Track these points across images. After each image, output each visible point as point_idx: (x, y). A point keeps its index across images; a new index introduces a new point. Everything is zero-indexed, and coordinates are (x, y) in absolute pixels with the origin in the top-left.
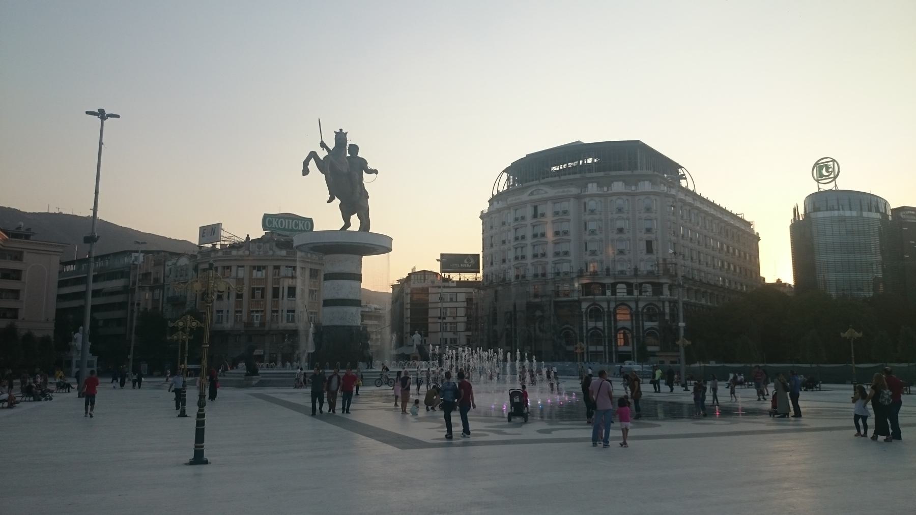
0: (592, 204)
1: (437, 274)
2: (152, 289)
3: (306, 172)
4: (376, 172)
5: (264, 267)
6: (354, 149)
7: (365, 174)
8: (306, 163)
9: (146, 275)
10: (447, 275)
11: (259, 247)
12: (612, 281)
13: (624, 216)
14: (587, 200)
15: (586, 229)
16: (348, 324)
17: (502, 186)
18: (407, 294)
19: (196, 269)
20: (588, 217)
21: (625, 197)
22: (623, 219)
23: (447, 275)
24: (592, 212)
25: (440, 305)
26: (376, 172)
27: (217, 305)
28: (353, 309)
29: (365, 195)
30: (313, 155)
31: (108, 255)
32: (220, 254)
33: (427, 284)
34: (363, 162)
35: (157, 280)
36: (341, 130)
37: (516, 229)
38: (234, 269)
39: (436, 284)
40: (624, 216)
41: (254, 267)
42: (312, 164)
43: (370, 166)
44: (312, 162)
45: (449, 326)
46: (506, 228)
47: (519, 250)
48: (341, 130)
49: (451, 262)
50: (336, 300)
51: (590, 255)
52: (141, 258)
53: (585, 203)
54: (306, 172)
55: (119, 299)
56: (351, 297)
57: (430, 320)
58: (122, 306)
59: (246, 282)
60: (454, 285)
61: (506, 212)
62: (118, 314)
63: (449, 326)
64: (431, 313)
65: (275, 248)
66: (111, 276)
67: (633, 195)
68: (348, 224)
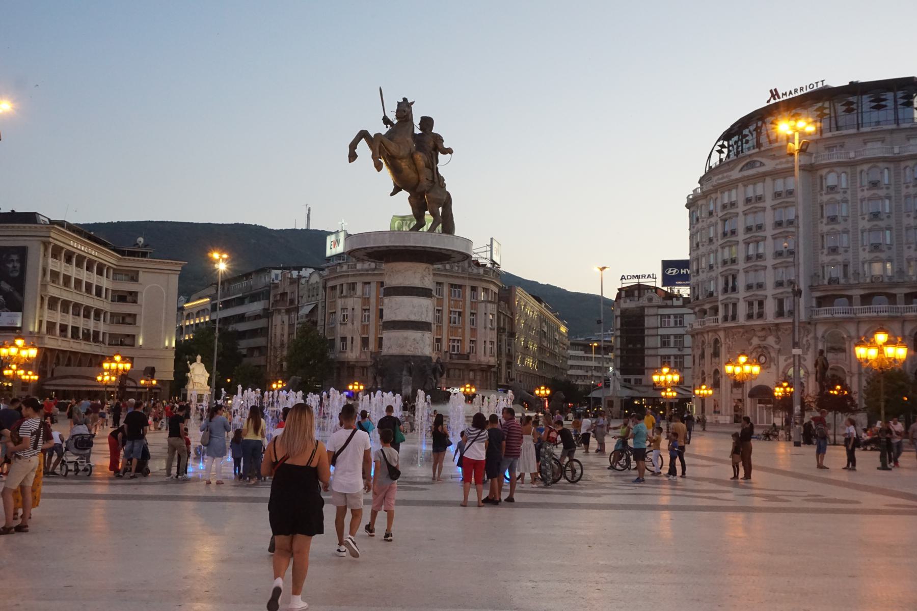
0: (831, 180)
1: (656, 288)
2: (288, 311)
3: (353, 157)
4: (449, 151)
6: (427, 123)
7: (440, 154)
8: (353, 146)
9: (284, 294)
10: (676, 290)
12: (862, 292)
13: (882, 193)
14: (824, 172)
15: (822, 216)
16: (409, 353)
17: (715, 160)
18: (616, 317)
19: (325, 288)
20: (825, 198)
21: (882, 165)
22: (880, 198)
23: (676, 290)
24: (832, 189)
25: (661, 331)
26: (449, 151)
27: (340, 331)
28: (417, 335)
29: (438, 182)
30: (363, 134)
31: (250, 274)
32: (345, 267)
33: (644, 302)
34: (438, 139)
35: (292, 301)
36: (405, 99)
37: (725, 221)
38: (359, 288)
39: (655, 302)
40: (882, 193)
42: (363, 148)
43: (446, 145)
44: (363, 145)
45: (672, 358)
46: (713, 220)
47: (727, 250)
48: (405, 99)
49: (674, 270)
50: (394, 322)
51: (829, 254)
52: (280, 278)
53: (821, 177)
54: (353, 157)
55: (261, 323)
56: (413, 318)
57: (646, 352)
58: (263, 332)
59: (373, 300)
60: (680, 303)
61: (713, 196)
62: (259, 341)
63: (672, 358)
64: (649, 342)
66: (254, 298)
67: (896, 160)
68: (421, 223)
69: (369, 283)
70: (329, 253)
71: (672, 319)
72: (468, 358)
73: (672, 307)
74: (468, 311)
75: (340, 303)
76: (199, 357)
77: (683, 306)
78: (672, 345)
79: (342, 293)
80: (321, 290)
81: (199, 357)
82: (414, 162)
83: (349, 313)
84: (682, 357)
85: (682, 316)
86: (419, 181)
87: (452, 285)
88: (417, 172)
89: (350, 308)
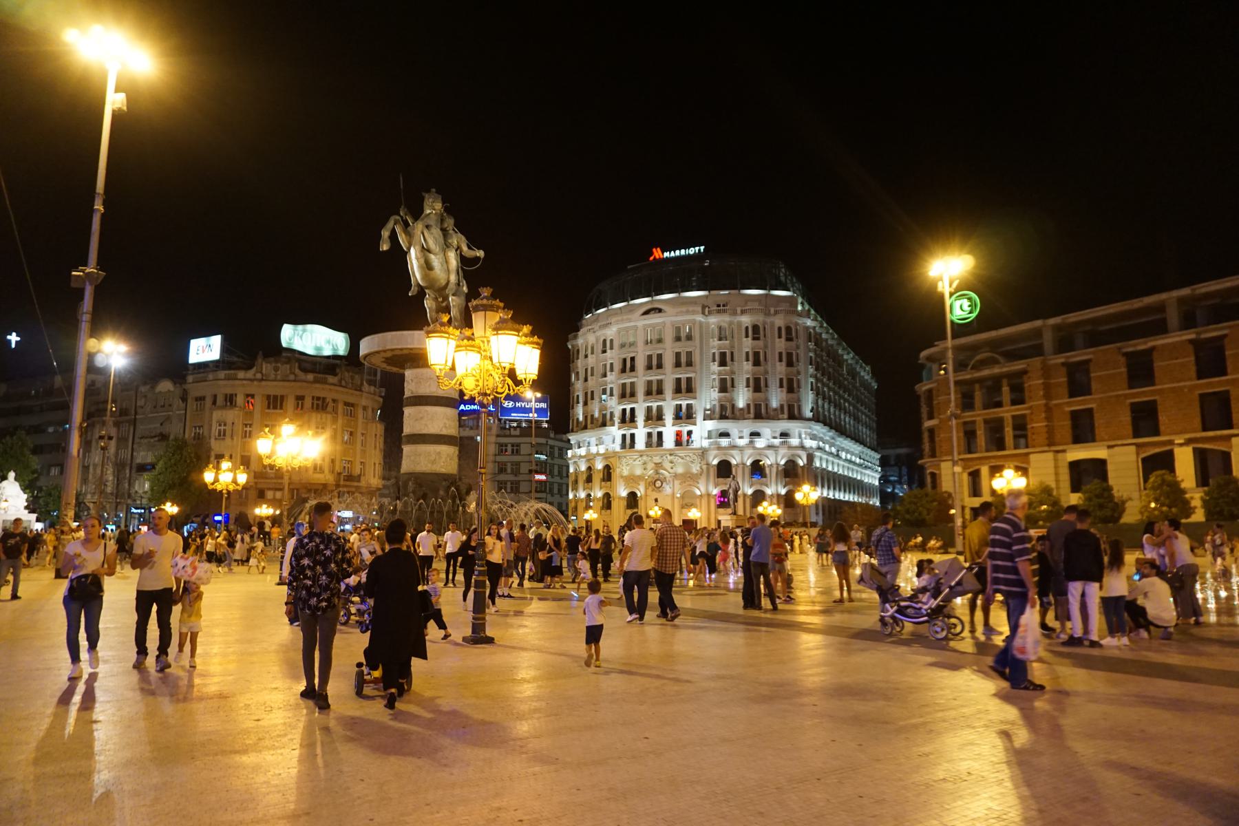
5: (282, 397)
11: (276, 369)
19: (184, 399)
38: (240, 400)
41: (268, 397)
45: (509, 485)
56: (444, 432)
65: (297, 371)
69: (253, 396)
70: (194, 358)
71: (509, 448)
72: (359, 481)
73: (510, 436)
74: (359, 434)
75: (217, 415)
76: (12, 475)
77: (521, 436)
78: (509, 470)
79: (214, 403)
80: (178, 402)
81: (12, 475)
82: (447, 262)
83: (228, 428)
84: (518, 482)
85: (518, 445)
86: (448, 282)
87: (346, 404)
88: (448, 271)
89: (229, 422)
